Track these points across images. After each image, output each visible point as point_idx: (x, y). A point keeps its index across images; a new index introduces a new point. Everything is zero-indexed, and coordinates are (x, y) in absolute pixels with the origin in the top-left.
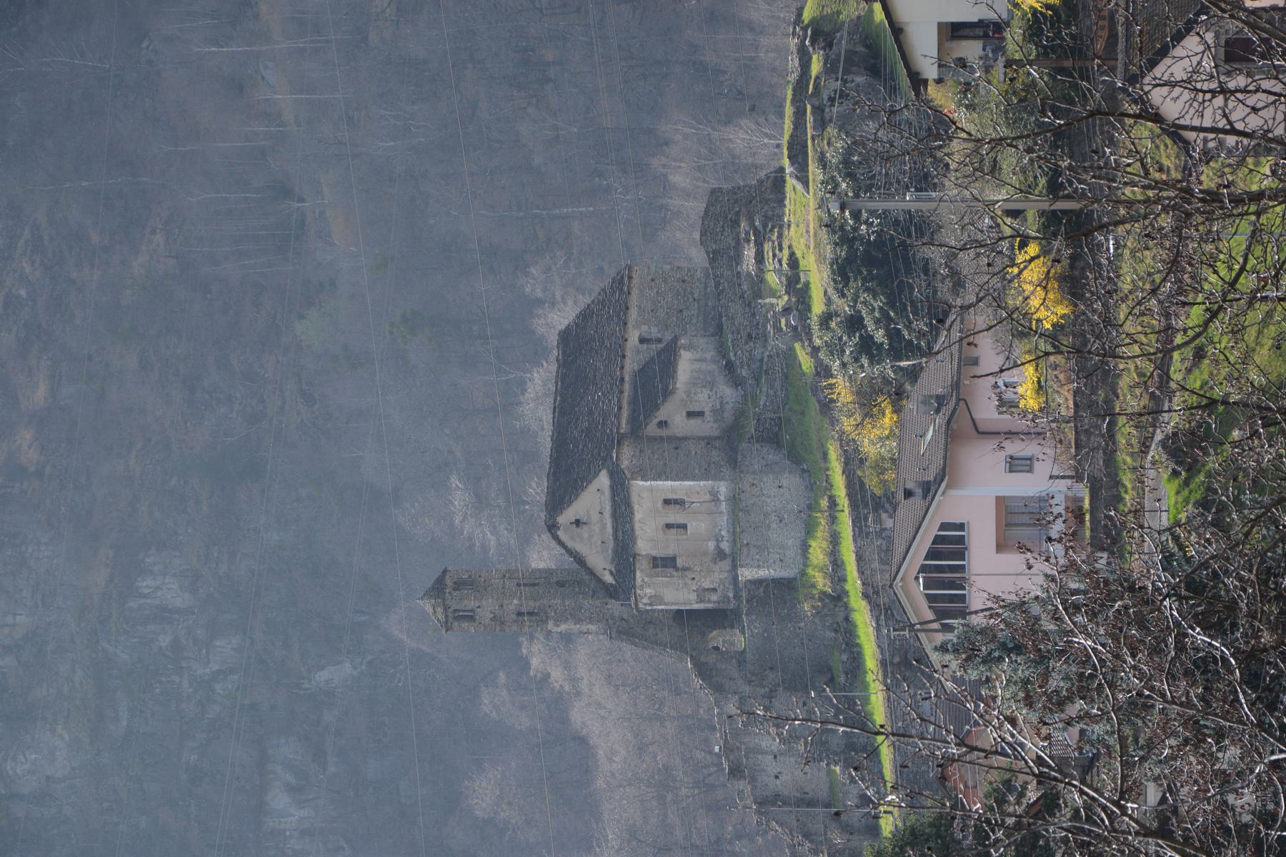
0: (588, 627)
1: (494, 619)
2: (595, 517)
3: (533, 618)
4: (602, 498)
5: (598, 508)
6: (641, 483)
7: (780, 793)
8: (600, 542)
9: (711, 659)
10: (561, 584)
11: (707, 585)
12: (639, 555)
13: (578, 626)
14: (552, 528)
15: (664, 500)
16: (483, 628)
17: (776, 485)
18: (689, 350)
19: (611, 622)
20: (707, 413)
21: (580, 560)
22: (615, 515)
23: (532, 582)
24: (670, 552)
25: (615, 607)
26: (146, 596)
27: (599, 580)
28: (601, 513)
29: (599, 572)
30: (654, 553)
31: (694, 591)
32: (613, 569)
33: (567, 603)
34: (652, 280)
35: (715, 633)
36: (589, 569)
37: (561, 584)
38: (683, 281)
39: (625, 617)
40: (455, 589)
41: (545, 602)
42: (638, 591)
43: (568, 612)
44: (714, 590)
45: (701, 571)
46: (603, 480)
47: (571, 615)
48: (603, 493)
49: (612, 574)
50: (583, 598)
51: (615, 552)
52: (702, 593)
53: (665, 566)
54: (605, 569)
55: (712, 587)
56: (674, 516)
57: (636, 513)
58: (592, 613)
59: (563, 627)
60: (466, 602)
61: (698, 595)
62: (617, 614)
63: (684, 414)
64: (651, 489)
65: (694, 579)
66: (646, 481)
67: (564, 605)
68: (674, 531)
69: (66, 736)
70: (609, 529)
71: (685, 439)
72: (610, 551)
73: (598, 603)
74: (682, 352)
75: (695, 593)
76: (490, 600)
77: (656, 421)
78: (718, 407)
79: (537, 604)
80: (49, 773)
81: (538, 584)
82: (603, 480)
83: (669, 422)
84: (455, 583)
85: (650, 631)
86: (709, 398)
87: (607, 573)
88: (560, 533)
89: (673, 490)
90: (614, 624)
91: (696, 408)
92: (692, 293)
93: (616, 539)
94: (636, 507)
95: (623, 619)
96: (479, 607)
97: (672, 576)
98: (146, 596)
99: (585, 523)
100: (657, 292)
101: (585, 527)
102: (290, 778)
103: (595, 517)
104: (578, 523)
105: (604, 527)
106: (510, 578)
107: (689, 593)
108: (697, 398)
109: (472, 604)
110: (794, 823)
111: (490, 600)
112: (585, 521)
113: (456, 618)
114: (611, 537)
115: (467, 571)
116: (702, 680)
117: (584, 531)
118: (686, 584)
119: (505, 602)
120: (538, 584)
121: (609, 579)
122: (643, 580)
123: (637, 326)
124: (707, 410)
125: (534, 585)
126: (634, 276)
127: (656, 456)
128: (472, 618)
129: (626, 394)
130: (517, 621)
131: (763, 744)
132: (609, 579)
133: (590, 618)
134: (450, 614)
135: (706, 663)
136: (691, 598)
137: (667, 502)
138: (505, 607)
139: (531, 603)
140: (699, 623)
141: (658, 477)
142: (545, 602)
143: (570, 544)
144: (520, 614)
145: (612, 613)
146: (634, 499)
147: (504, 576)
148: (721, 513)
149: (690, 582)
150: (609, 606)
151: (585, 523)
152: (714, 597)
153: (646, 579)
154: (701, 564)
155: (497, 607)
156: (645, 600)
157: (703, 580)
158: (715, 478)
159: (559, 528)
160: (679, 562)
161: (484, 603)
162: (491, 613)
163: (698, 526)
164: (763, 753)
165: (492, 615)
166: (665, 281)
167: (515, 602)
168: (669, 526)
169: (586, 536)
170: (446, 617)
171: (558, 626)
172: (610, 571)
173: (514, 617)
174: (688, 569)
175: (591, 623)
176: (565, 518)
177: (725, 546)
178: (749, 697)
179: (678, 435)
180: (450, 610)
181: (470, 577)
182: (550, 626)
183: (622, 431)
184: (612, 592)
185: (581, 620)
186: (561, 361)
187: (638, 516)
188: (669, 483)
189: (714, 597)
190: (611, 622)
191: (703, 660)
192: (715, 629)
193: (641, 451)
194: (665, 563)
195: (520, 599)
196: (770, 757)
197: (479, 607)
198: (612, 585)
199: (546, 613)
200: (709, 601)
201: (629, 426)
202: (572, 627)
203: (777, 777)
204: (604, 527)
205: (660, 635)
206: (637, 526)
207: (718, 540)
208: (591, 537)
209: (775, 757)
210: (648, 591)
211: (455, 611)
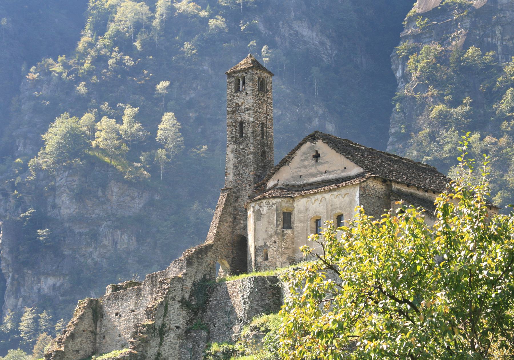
0: (231, 173)
1: (238, 106)
2: (322, 168)
3: (238, 134)
4: (339, 171)
5: (330, 169)
7: (104, 318)
8: (300, 174)
10: (264, 153)
11: (271, 252)
12: (293, 201)
13: (232, 166)
14: (313, 138)
15: (342, 215)
16: (230, 98)
19: (236, 190)
21: (285, 162)
23: (265, 133)
24: (297, 224)
25: (248, 190)
26: (121, 237)
27: (269, 178)
28: (326, 172)
29: (276, 177)
30: (295, 212)
31: (265, 243)
33: (250, 156)
35: (228, 266)
36: (279, 169)
37: (264, 153)
39: (239, 199)
40: (259, 78)
41: (251, 141)
42: (264, 201)
43: (243, 158)
44: (266, 259)
47: (241, 160)
50: (254, 168)
54: (279, 180)
55: (269, 257)
57: (330, 194)
58: (242, 175)
60: (251, 84)
61: (261, 246)
62: (242, 193)
64: (351, 202)
65: (275, 242)
66: (360, 198)
68: (314, 226)
69: (74, 213)
70: (311, 180)
72: (294, 182)
73: (251, 178)
76: (252, 101)
79: (249, 135)
80: (62, 207)
81: (263, 137)
82: (356, 170)
84: (263, 79)
85: (229, 218)
87: (275, 182)
88: (308, 144)
90: (234, 193)
95: (238, 198)
96: (247, 94)
97: (277, 225)
98: (121, 237)
99: (317, 161)
101: (313, 162)
102: (58, 284)
103: (321, 168)
104: (317, 156)
105: (314, 175)
106: (267, 118)
107: (264, 239)
110: (82, 328)
111: (252, 101)
112: (319, 161)
114: (305, 182)
115: (271, 89)
118: (271, 236)
119: (251, 112)
120: (263, 137)
125: (263, 134)
126: (492, 211)
127: (376, 208)
128: (237, 90)
129: (417, 192)
130: (235, 121)
133: (238, 175)
134: (241, 74)
136: (259, 242)
137: (339, 218)
138: (247, 112)
139: (250, 130)
140: (235, 255)
142: (251, 141)
143: (299, 152)
144: (241, 123)
145: (242, 190)
147: (268, 115)
149: (273, 239)
150: (248, 187)
151: (317, 161)
152: (260, 259)
153: (275, 207)
154: (287, 248)
155: (246, 106)
156: (257, 207)
157: (275, 249)
161: (251, 97)
162: (242, 104)
164: (137, 304)
165: (240, 104)
167: (251, 119)
168: (318, 222)
169: (306, 163)
170: (239, 72)
172: (277, 184)
173: (239, 120)
174: (283, 235)
175: (235, 175)
176: (321, 146)
178: (183, 285)
180: (244, 74)
181: (268, 91)
182: (232, 146)
183: (393, 184)
185: (237, 167)
186: (418, 165)
187: (327, 196)
190: (236, 190)
191: (209, 254)
192: (231, 266)
193: (379, 198)
195: (253, 122)
197: (247, 94)
198: (266, 187)
199: (243, 142)
200: (256, 255)
201: (396, 190)
202: (232, 162)
204: (314, 175)
205: (226, 225)
208: (305, 167)
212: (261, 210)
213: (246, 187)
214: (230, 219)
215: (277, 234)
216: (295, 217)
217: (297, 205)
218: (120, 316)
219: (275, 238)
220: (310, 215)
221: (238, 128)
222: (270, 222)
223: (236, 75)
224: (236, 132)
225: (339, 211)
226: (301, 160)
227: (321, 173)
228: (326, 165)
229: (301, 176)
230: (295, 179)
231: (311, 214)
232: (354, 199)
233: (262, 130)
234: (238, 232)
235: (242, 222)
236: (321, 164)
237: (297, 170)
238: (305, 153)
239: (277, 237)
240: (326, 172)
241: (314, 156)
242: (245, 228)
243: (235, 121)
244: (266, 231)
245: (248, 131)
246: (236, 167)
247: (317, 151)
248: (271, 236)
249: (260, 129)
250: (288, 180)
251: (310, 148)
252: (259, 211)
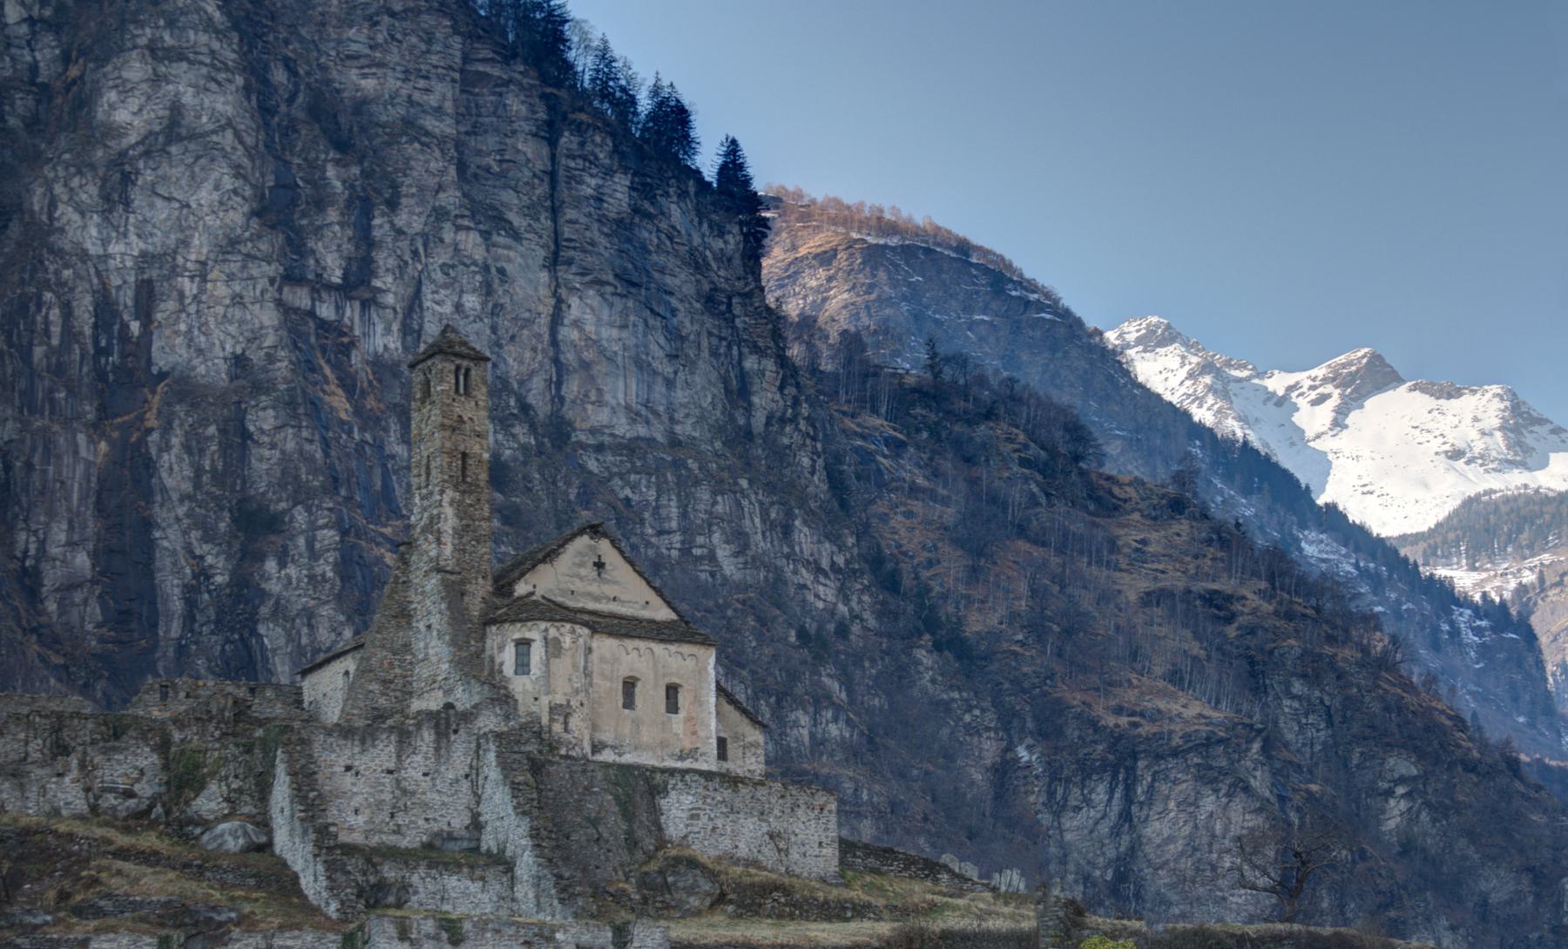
4: (637, 606)
5: (623, 597)
6: (712, 660)
8: (573, 588)
13: (451, 532)
17: (824, 840)
22: (613, 616)
28: (614, 599)
31: (569, 701)
32: (534, 598)
46: (663, 614)
47: (468, 526)
48: (644, 608)
54: (534, 586)
56: (650, 697)
57: (662, 646)
59: (449, 511)
61: (561, 705)
64: (702, 671)
75: (565, 703)
82: (663, 614)
87: (530, 588)
88: (584, 541)
94: (673, 648)
96: (477, 405)
103: (610, 590)
104: (599, 565)
105: (597, 599)
107: (565, 694)
108: (748, 754)
113: (458, 368)
114: (580, 605)
121: (521, 589)
131: (418, 758)
134: (465, 363)
136: (558, 696)
137: (672, 691)
146: (686, 649)
150: (480, 581)
151: (599, 575)
156: (553, 632)
159: (592, 538)
168: (629, 685)
169: (583, 572)
171: (451, 505)
172: (532, 594)
173: (462, 448)
175: (455, 549)
196: (391, 766)
197: (477, 405)
199: (471, 493)
200: (552, 720)
203: (348, 768)
204: (597, 599)
206: (642, 644)
208: (581, 578)
209: (390, 772)
210: (567, 641)
211: (468, 371)
212: (562, 639)
213: (476, 578)
217: (599, 647)
218: (357, 774)
220: (621, 673)
226: (574, 564)
228: (616, 587)
229: (573, 592)
230: (563, 592)
231: (624, 672)
232: (706, 669)
236: (608, 582)
237: (567, 578)
238: (580, 553)
240: (614, 599)
241: (595, 564)
244: (570, 680)
246: (459, 533)
248: (577, 692)
250: (551, 590)
251: (591, 547)
252: (557, 641)
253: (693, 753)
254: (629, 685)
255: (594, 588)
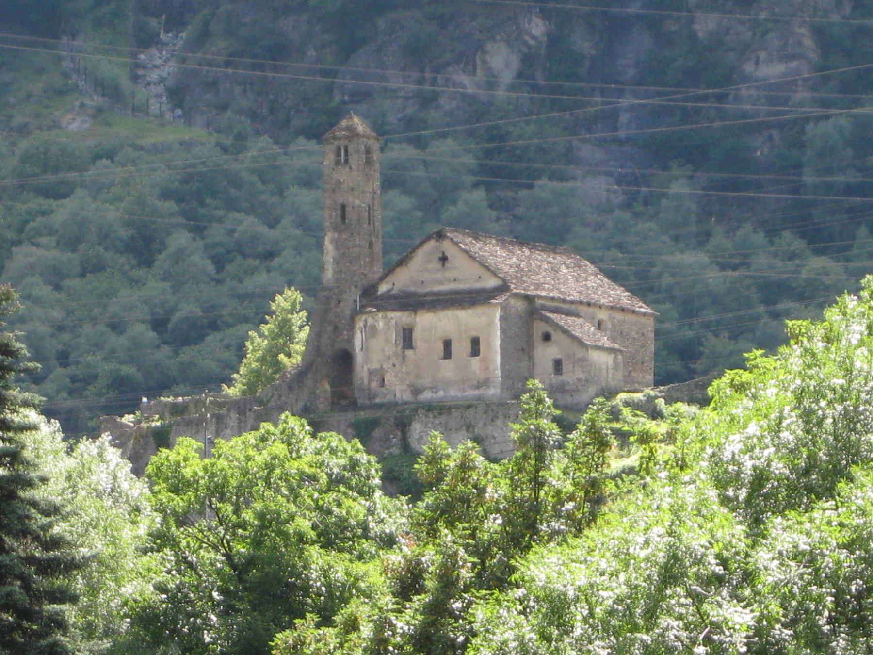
0: (330, 269)
2: (449, 274)
3: (339, 219)
9: (309, 382)
11: (389, 378)
13: (332, 260)
18: (614, 362)
19: (336, 291)
20: (560, 378)
25: (353, 295)
28: (455, 280)
31: (382, 367)
32: (394, 292)
34: (643, 334)
36: (394, 269)
38: (643, 363)
39: (342, 304)
40: (365, 147)
45: (402, 372)
47: (344, 254)
48: (476, 281)
49: (389, 291)
51: (414, 295)
52: (379, 375)
53: (404, 340)
54: (394, 284)
55: (386, 382)
56: (461, 348)
62: (344, 296)
63: (559, 356)
64: (490, 323)
65: (394, 365)
67: (353, 248)
70: (437, 288)
71: (531, 358)
74: (613, 356)
77: (550, 330)
78: (568, 388)
81: (369, 223)
83: (549, 343)
84: (370, 147)
86: (577, 379)
87: (389, 286)
88: (432, 243)
89: (489, 346)
91: (566, 366)
92: (634, 370)
93: (425, 295)
96: (351, 168)
97: (397, 345)
99: (443, 265)
100: (634, 339)
101: (439, 266)
104: (444, 259)
105: (441, 283)
109: (354, 161)
114: (428, 289)
116: (296, 373)
117: (435, 265)
120: (369, 223)
122: (392, 318)
123: (612, 318)
124: (564, 378)
128: (338, 163)
132: (383, 288)
135: (307, 378)
141: (503, 331)
144: (343, 207)
148: (464, 391)
149: (391, 362)
150: (353, 289)
151: (443, 265)
152: (374, 385)
153: (393, 322)
156: (370, 321)
158: (503, 384)
159: (437, 241)
160: (409, 353)
163: (447, 369)
165: (342, 180)
166: (643, 346)
168: (447, 344)
169: (430, 266)
172: (392, 289)
174: (404, 358)
177: (426, 396)
179: (535, 351)
180: (347, 142)
183: (536, 300)
184: (369, 293)
188: (498, 342)
189: (374, 385)
191: (310, 375)
192: (331, 387)
194: (407, 338)
197: (351, 168)
198: (376, 291)
207: (433, 388)
210: (381, 324)
212: (377, 324)
213: (350, 289)
214: (330, 328)
215: (396, 355)
216: (417, 335)
219: (393, 360)
221: (339, 211)
222: (387, 341)
223: (336, 142)
224: (336, 216)
225: (474, 334)
227: (449, 281)
232: (493, 321)
233: (369, 213)
234: (340, 345)
235: (345, 332)
239: (397, 359)
240: (455, 280)
242: (350, 340)
243: (335, 202)
245: (351, 215)
246: (337, 261)
247: (443, 253)
248: (389, 358)
249: (367, 213)
253: (485, 383)
254: (447, 344)
255: (439, 276)
